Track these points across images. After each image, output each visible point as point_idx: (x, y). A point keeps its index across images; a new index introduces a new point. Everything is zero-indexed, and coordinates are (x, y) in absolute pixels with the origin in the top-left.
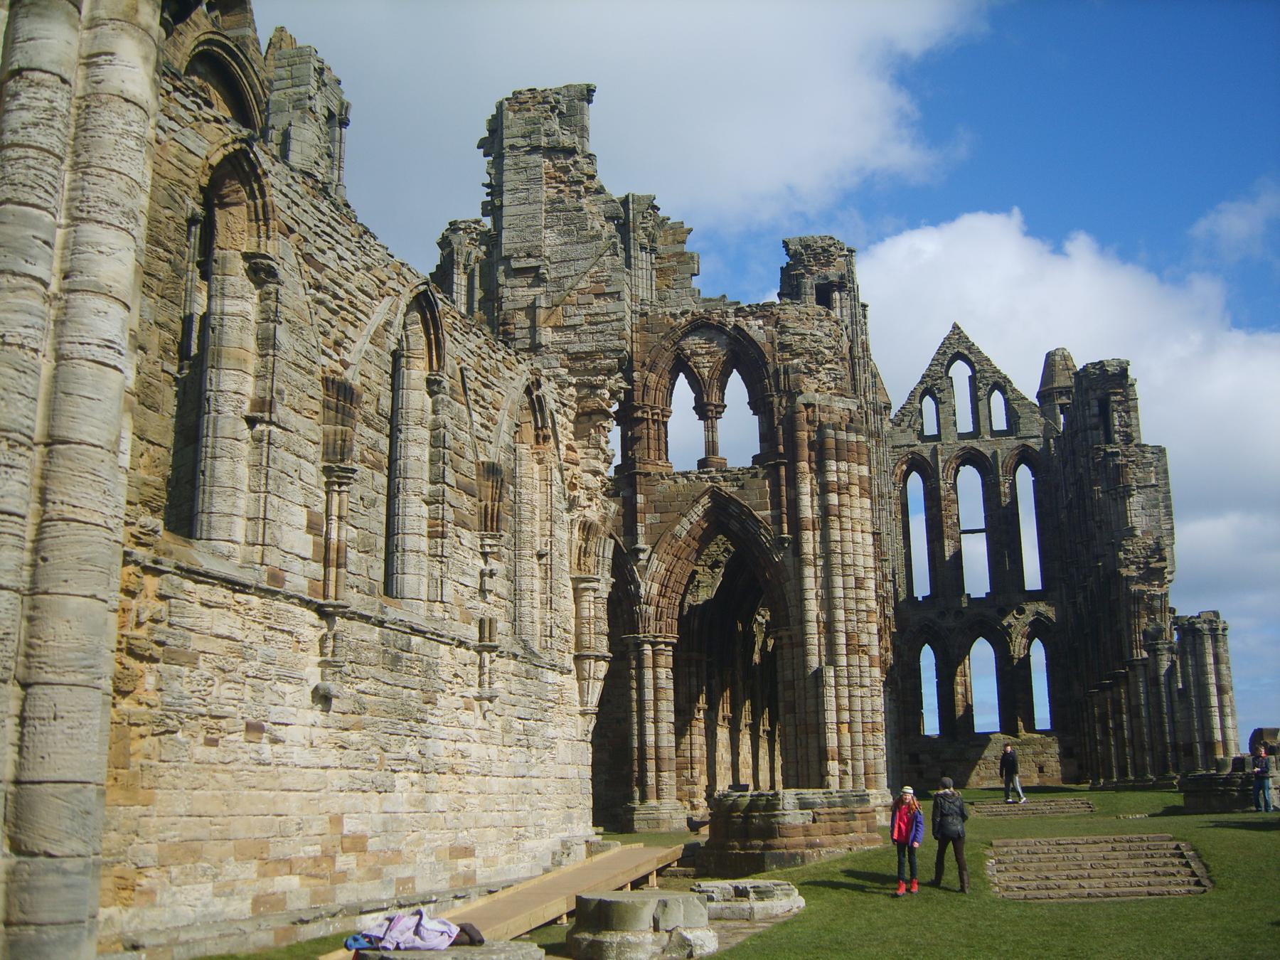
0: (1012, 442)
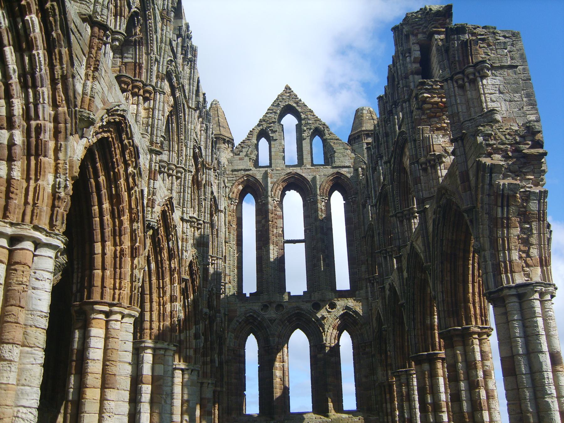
0: (329, 170)
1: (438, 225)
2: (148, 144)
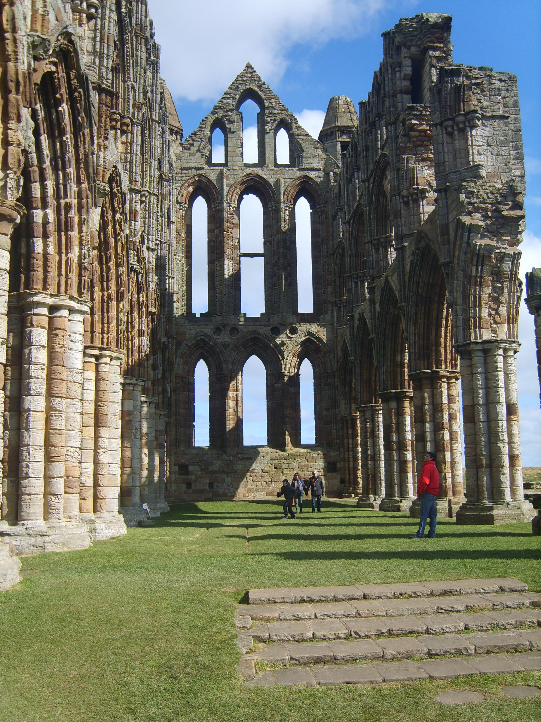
0: (295, 173)
1: (416, 266)
2: (128, 183)
